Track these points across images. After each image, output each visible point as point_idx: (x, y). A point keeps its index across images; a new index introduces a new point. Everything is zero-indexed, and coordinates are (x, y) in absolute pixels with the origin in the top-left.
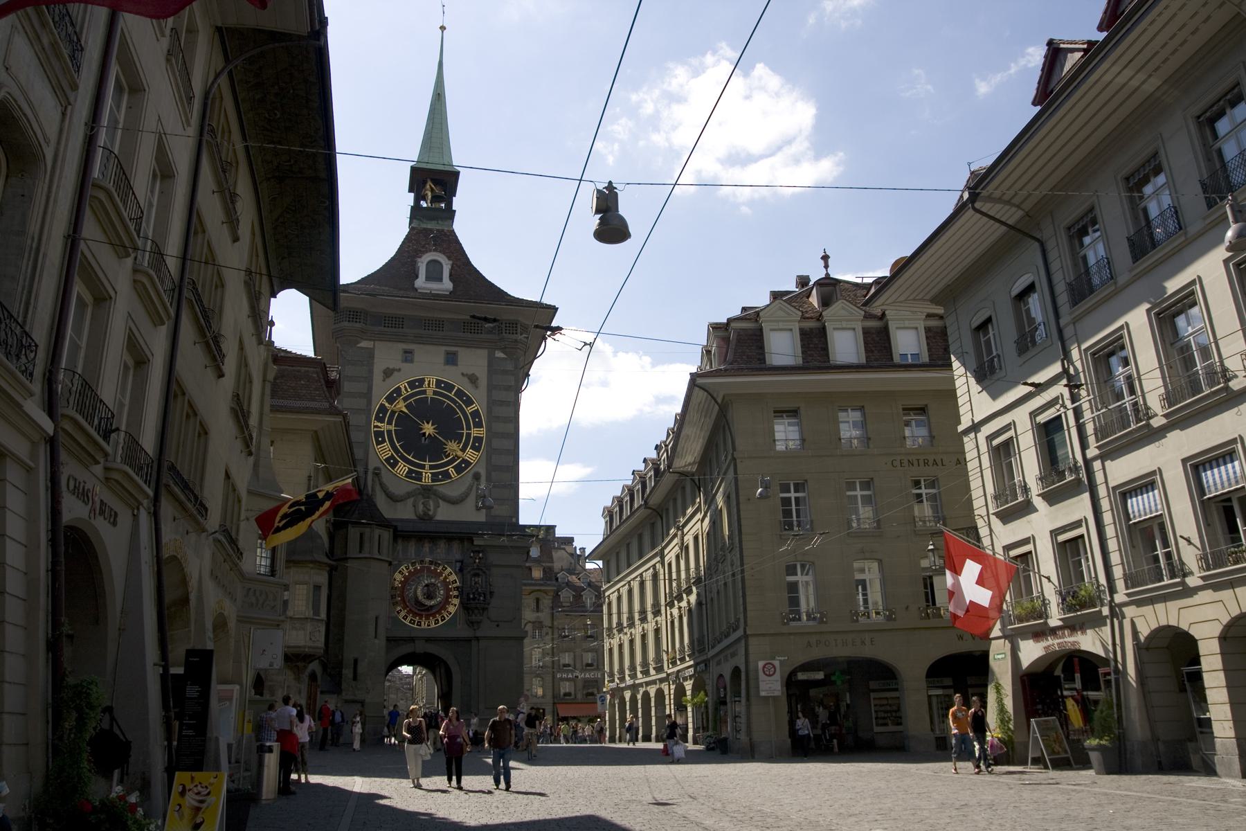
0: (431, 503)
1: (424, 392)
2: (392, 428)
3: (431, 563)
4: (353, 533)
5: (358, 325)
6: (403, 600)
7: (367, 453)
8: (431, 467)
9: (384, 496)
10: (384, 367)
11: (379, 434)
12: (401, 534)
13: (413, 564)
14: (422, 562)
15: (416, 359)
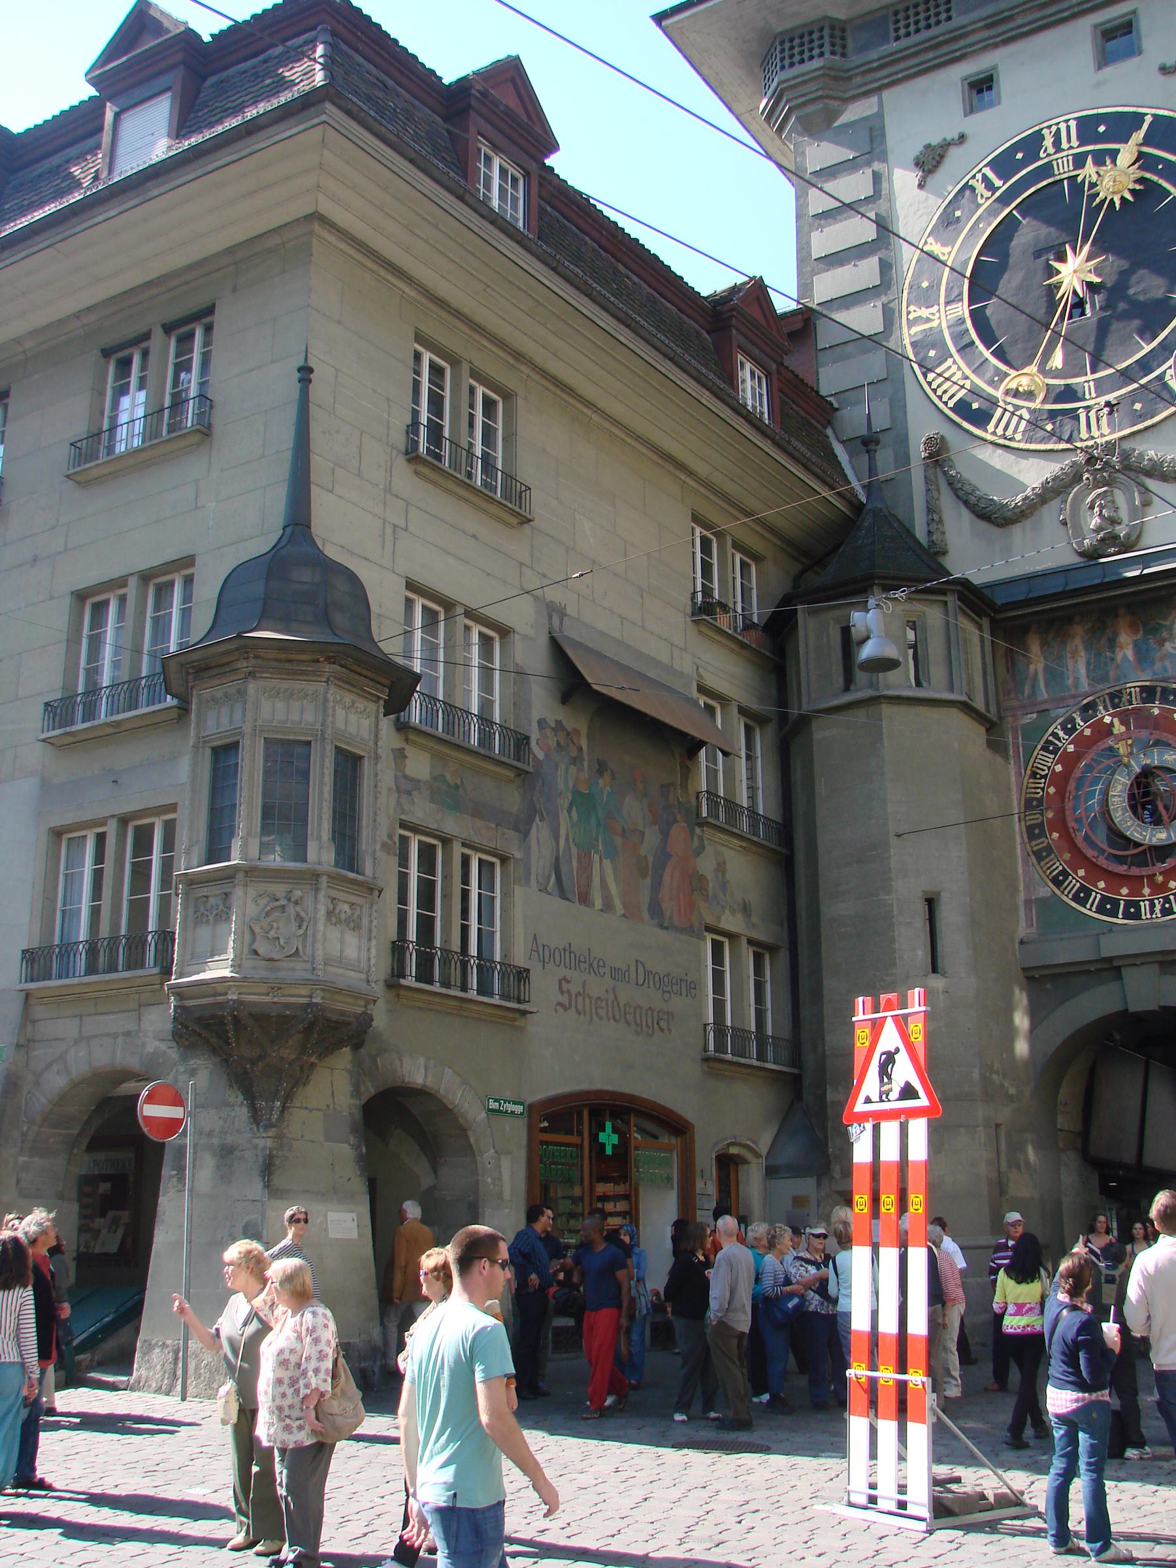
0: (1120, 497)
1: (1047, 170)
2: (962, 309)
3: (1148, 693)
4: (813, 632)
5: (817, 63)
6: (1067, 836)
7: (898, 405)
8: (1101, 387)
9: (965, 514)
10: (916, 149)
11: (931, 340)
12: (1019, 618)
13: (1088, 709)
14: (1115, 698)
15: (1005, 84)
